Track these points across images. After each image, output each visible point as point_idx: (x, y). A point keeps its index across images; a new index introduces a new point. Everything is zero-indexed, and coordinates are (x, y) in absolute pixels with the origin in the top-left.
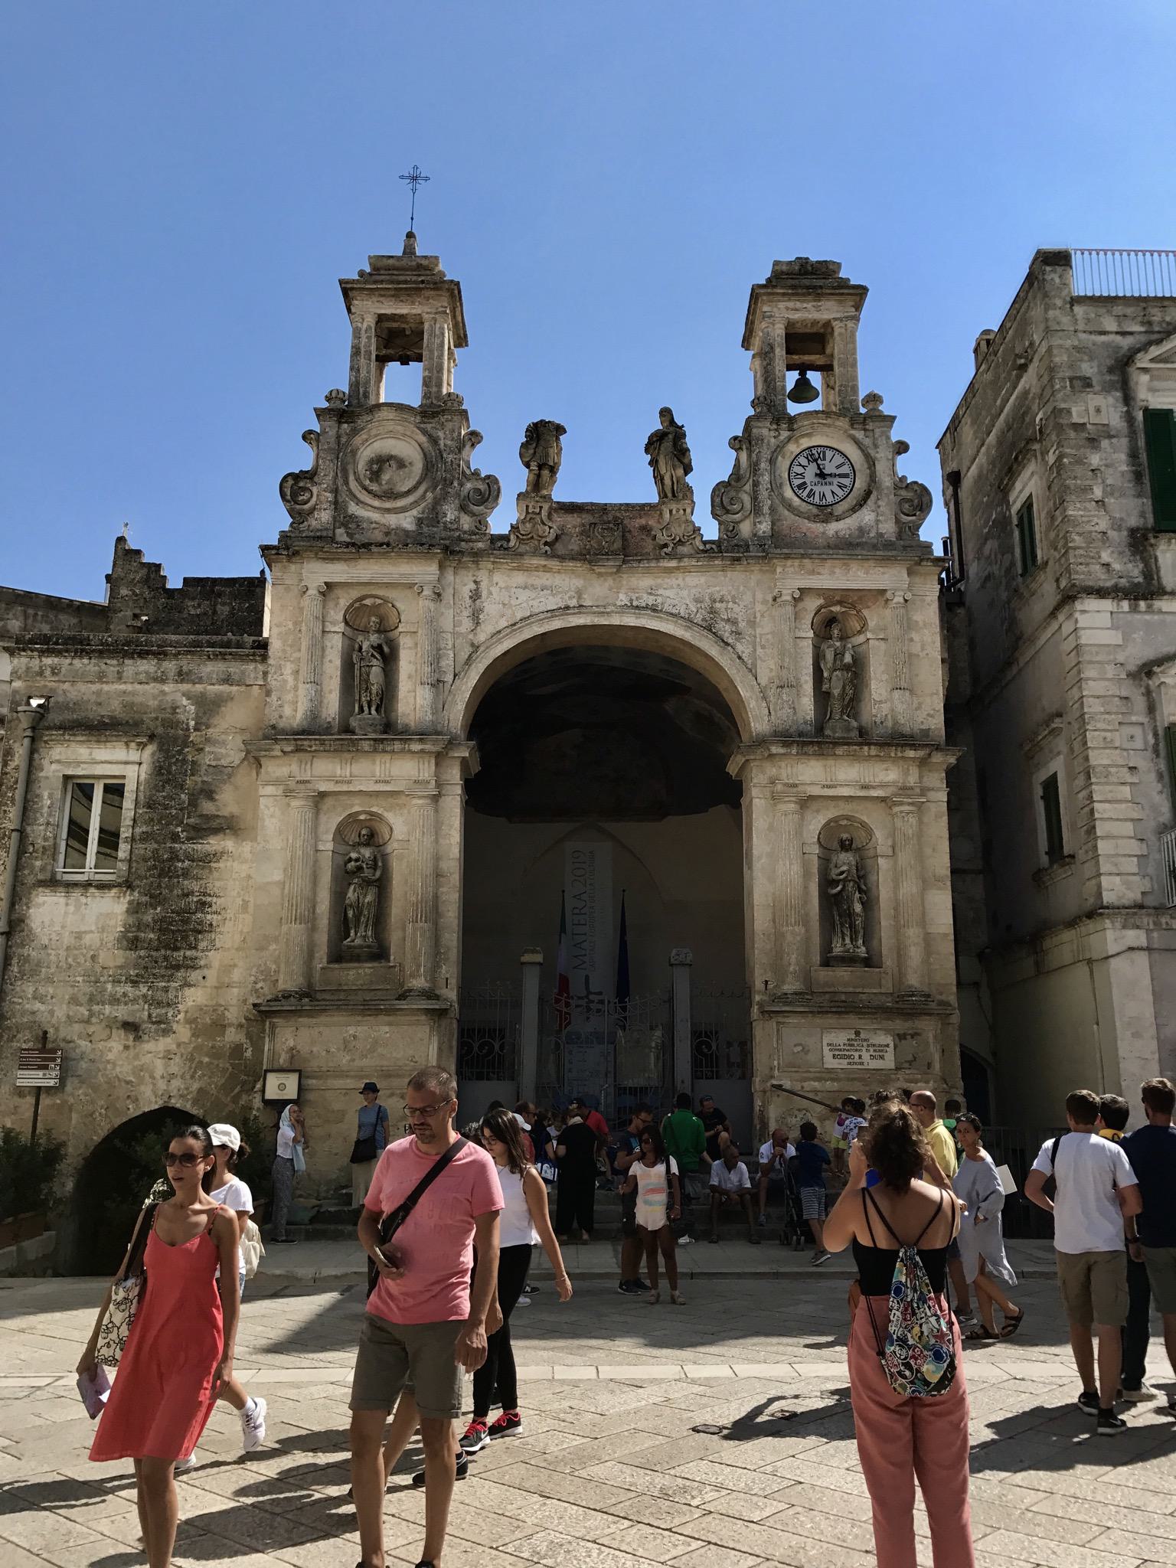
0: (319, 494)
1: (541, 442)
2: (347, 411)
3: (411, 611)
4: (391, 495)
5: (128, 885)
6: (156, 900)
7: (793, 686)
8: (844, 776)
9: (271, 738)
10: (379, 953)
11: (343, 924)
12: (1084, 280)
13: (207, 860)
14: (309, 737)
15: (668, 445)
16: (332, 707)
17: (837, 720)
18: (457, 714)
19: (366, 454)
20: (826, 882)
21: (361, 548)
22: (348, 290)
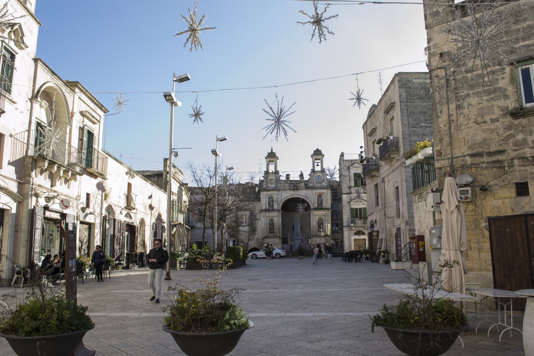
0: (264, 183)
1: (288, 175)
2: (267, 172)
3: (275, 197)
4: (272, 183)
5: (248, 226)
6: (251, 227)
7: (315, 203)
8: (321, 213)
9: (261, 211)
10: (274, 232)
11: (270, 230)
12: (346, 158)
13: (256, 223)
14: (266, 210)
15: (301, 175)
16: (267, 207)
17: (320, 208)
18: (280, 208)
19: (269, 178)
20: (318, 224)
21: (269, 190)
22: (266, 158)
